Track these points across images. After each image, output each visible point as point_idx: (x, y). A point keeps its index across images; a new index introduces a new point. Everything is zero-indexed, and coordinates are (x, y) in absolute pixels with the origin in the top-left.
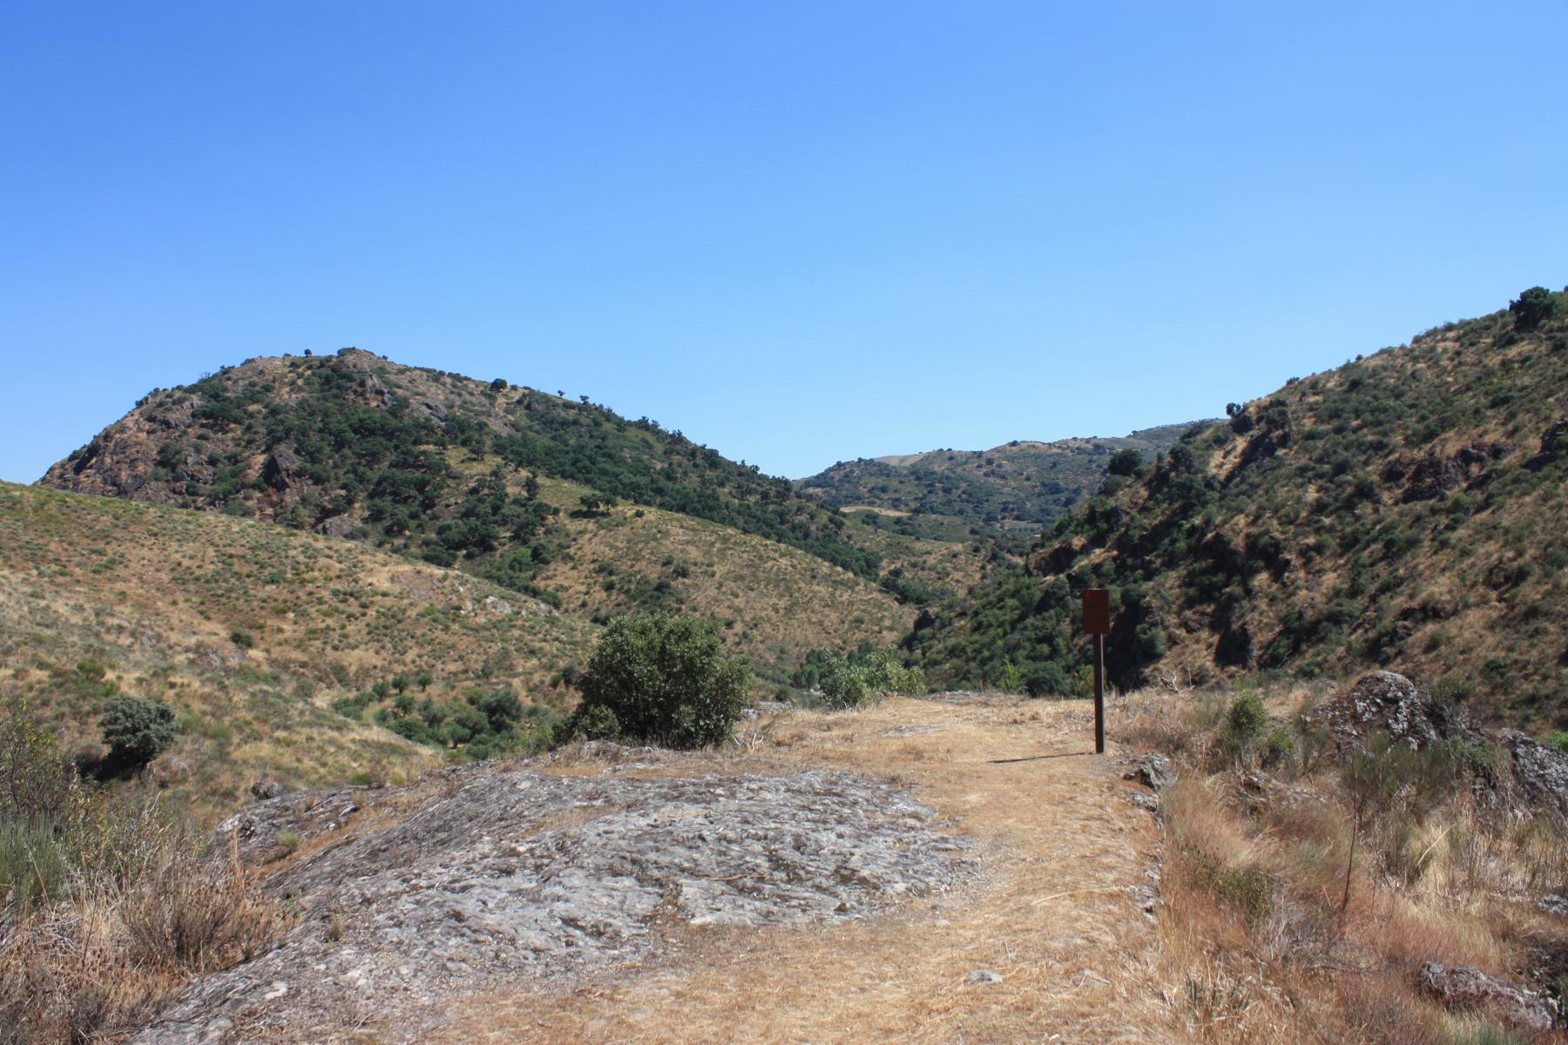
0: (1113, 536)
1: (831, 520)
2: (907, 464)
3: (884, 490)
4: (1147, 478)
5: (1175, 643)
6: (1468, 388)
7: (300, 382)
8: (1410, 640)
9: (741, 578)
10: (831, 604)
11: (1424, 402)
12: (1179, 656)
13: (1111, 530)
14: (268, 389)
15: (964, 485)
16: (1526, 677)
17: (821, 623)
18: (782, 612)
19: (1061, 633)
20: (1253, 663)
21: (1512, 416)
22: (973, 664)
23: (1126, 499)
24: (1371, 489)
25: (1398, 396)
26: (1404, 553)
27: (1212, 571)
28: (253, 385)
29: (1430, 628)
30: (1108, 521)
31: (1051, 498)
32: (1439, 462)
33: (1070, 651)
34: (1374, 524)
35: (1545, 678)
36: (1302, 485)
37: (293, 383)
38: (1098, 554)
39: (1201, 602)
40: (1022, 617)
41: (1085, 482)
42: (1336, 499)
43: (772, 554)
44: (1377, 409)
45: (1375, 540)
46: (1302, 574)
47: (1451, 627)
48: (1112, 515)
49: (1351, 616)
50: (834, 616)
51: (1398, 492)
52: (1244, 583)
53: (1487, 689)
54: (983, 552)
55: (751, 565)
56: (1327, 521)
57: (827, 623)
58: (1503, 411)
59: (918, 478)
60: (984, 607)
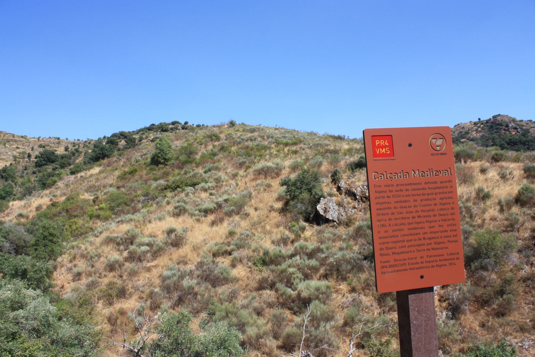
7: (479, 129)
14: (467, 133)
28: (461, 132)
37: (476, 130)
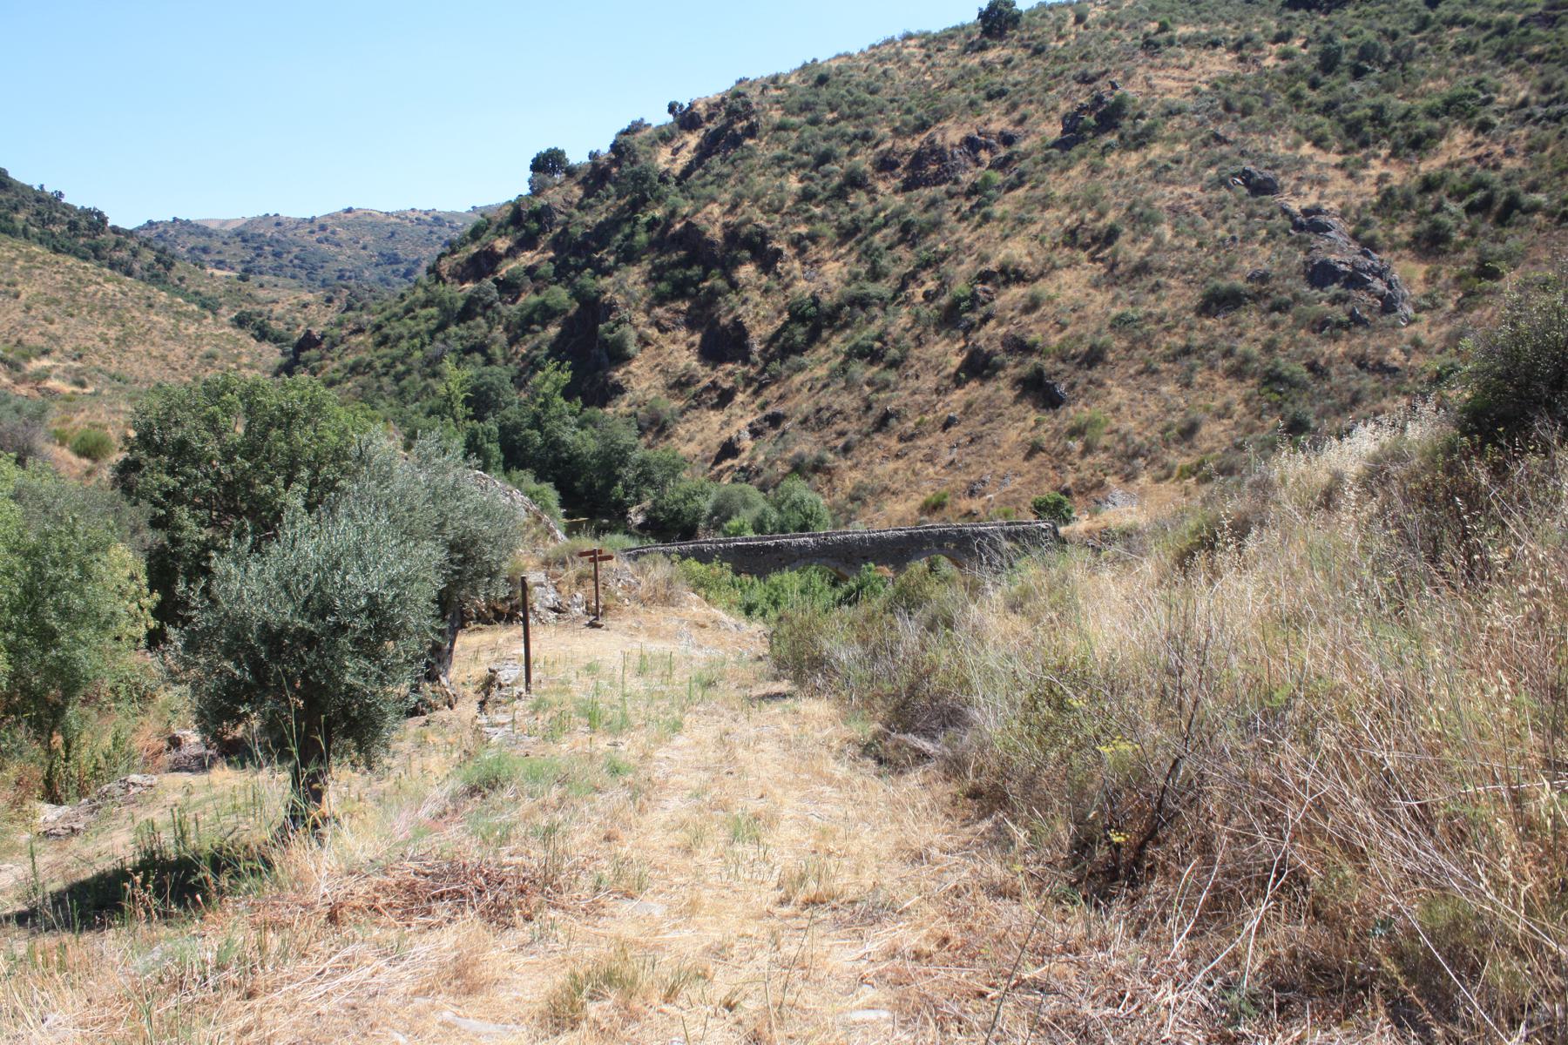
0: (547, 238)
1: (158, 260)
2: (229, 228)
3: (205, 250)
4: (580, 177)
5: (647, 344)
6: (952, 85)
8: (997, 303)
9: (57, 302)
10: (175, 336)
11: (906, 97)
12: (654, 357)
13: (542, 231)
15: (296, 250)
16: (1168, 329)
17: (164, 358)
18: (113, 343)
19: (494, 341)
20: (755, 357)
21: (1014, 106)
22: (386, 380)
23: (559, 198)
24: (864, 179)
25: (872, 93)
26: (927, 235)
27: (687, 263)
29: (1016, 292)
30: (538, 220)
31: (389, 268)
32: (942, 149)
33: (508, 360)
34: (876, 214)
35: (1190, 328)
36: (783, 174)
38: (528, 258)
39: (674, 298)
40: (442, 327)
41: (426, 254)
42: (824, 188)
43: (94, 278)
44: (855, 102)
45: (885, 225)
46: (797, 264)
47: (1045, 287)
48: (543, 215)
49: (882, 299)
50: (180, 350)
51: (897, 182)
52: (727, 275)
53: (1125, 344)
54: (337, 303)
55: (68, 287)
56: (818, 211)
57: (171, 358)
58: (1002, 105)
59: (244, 240)
60: (388, 320)
